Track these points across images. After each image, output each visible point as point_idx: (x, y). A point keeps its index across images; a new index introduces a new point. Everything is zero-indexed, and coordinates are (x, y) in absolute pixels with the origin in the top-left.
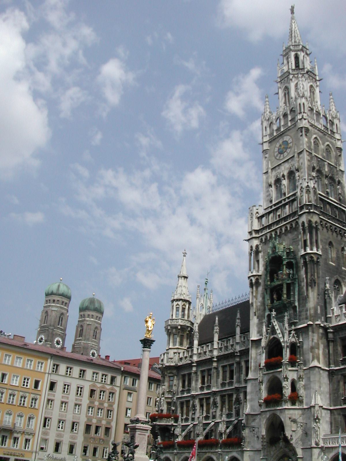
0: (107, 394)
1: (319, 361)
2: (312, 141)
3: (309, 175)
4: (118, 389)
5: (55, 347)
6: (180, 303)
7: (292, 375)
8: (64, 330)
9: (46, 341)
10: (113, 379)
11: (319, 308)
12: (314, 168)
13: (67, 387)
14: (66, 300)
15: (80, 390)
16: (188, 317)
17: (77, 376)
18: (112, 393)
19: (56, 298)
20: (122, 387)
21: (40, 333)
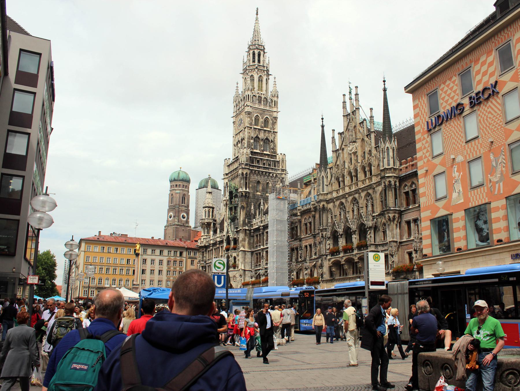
0: (178, 263)
1: (244, 247)
2: (253, 119)
3: (249, 142)
4: (184, 259)
5: (182, 221)
6: (207, 209)
7: (234, 254)
8: (188, 206)
9: (174, 217)
10: (181, 254)
11: (247, 220)
12: (252, 138)
13: (153, 261)
14: (185, 184)
15: (161, 262)
16: (212, 216)
17: (159, 254)
18: (181, 262)
19: (178, 183)
20: (187, 257)
21: (169, 211)
